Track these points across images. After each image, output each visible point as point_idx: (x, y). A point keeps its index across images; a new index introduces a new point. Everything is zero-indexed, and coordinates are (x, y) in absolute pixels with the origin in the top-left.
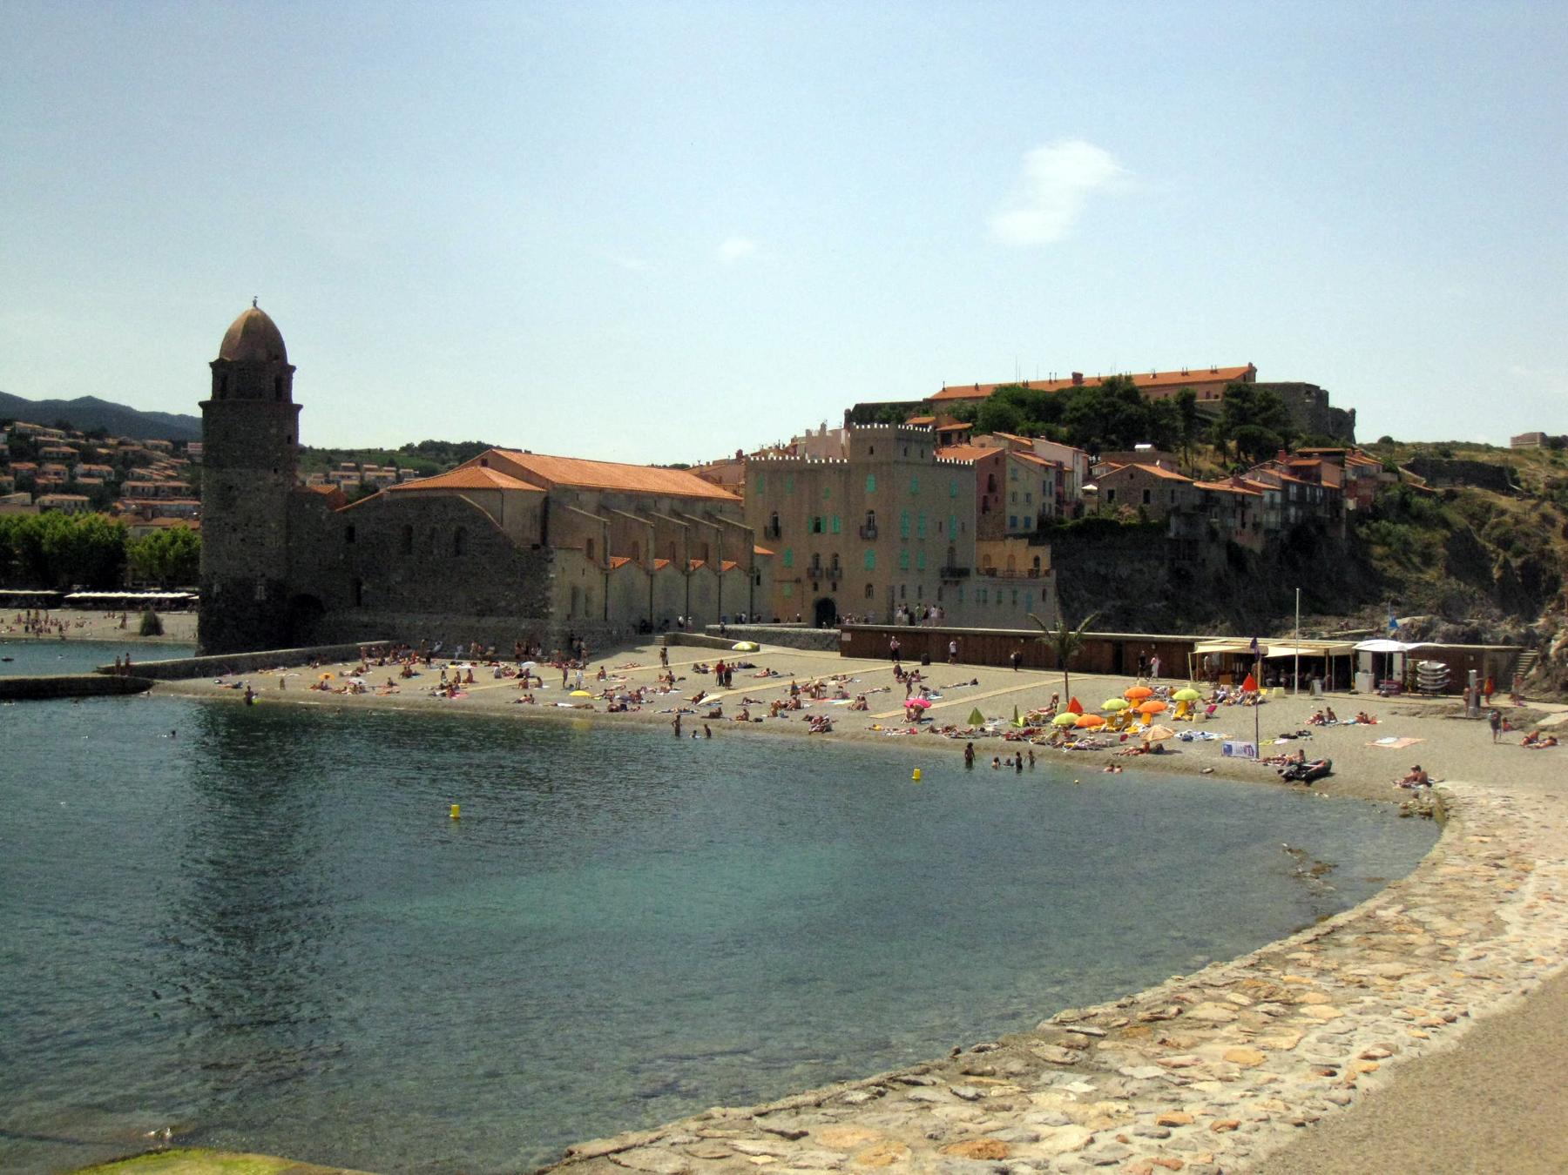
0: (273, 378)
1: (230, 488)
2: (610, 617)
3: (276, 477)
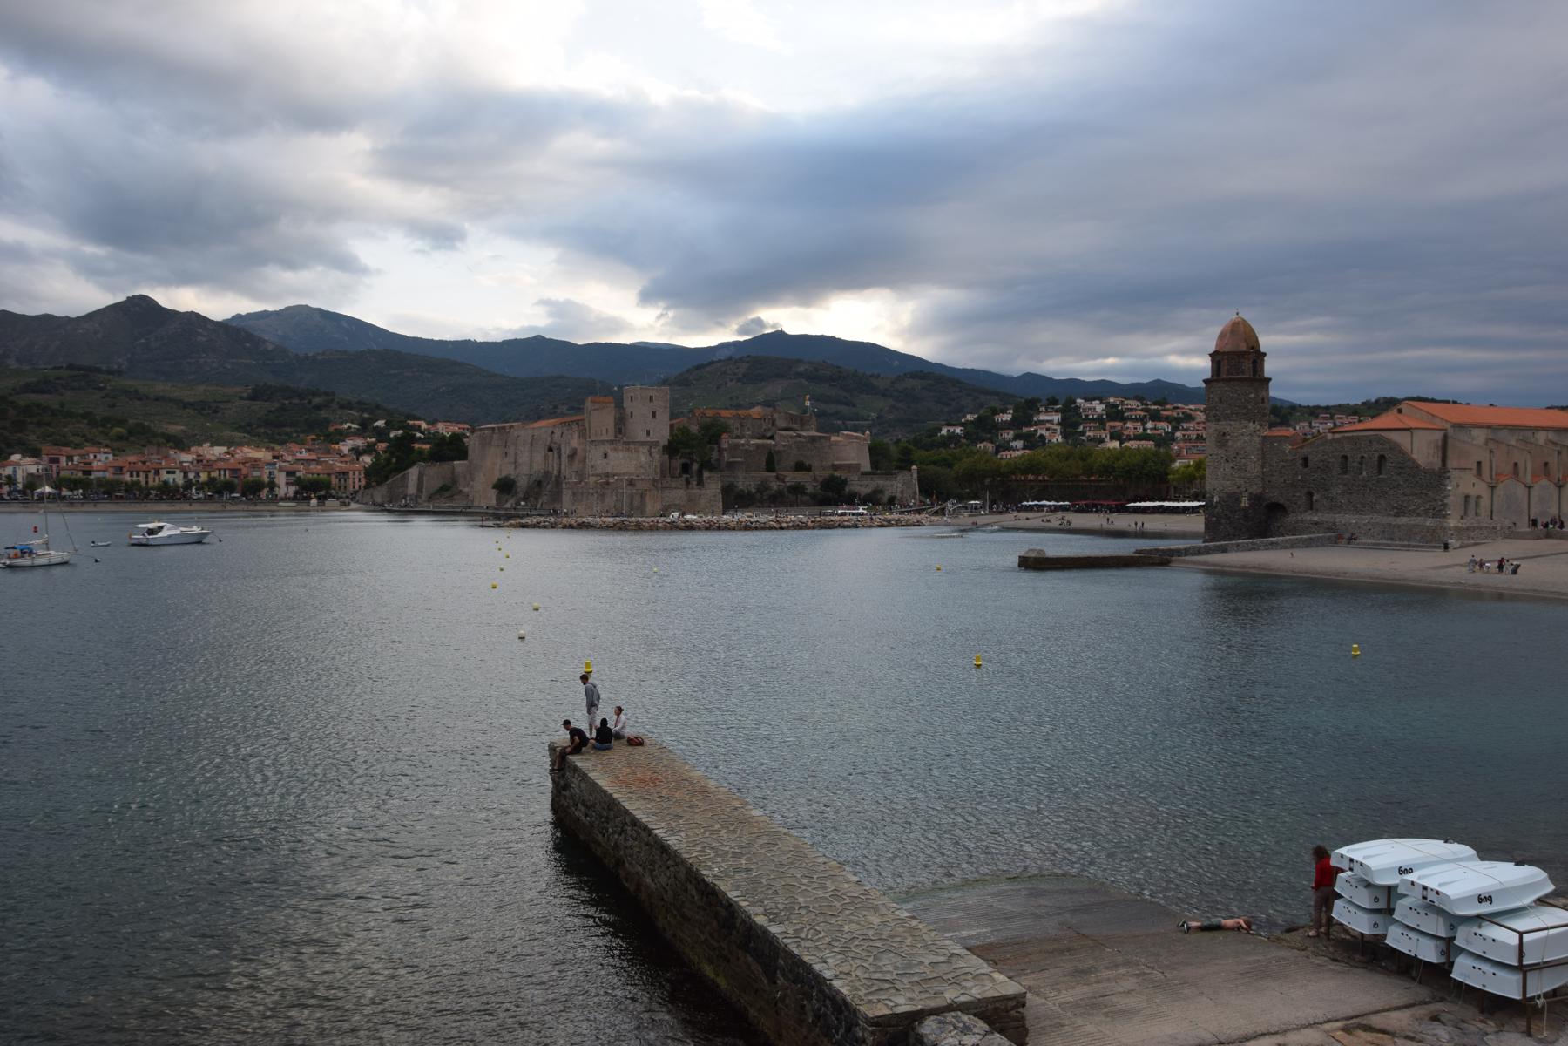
0: (1251, 361)
1: (1224, 434)
2: (1494, 517)
3: (1254, 426)
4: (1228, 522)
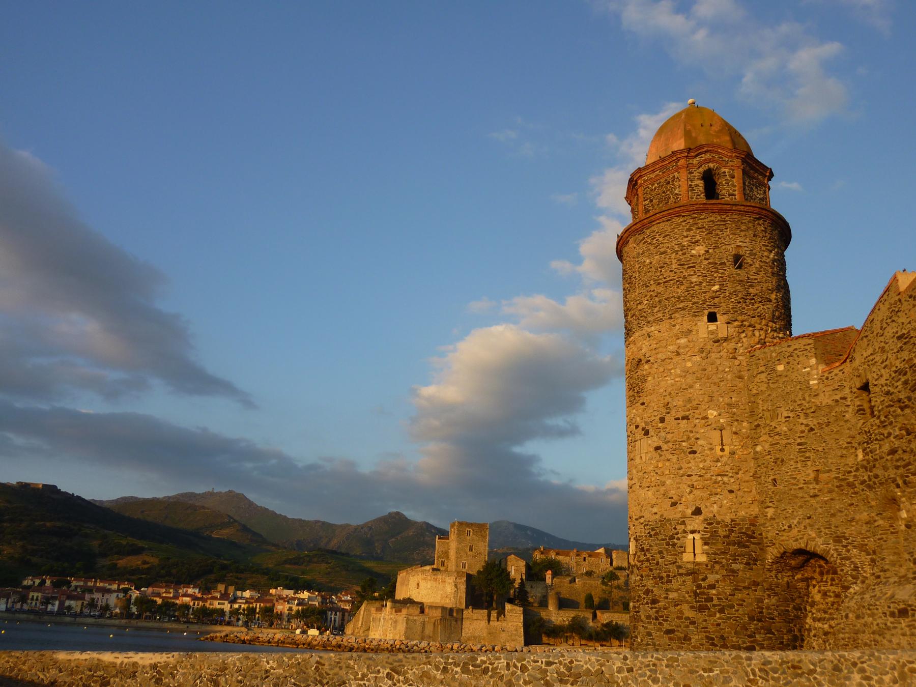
3: (712, 326)
4: (652, 613)
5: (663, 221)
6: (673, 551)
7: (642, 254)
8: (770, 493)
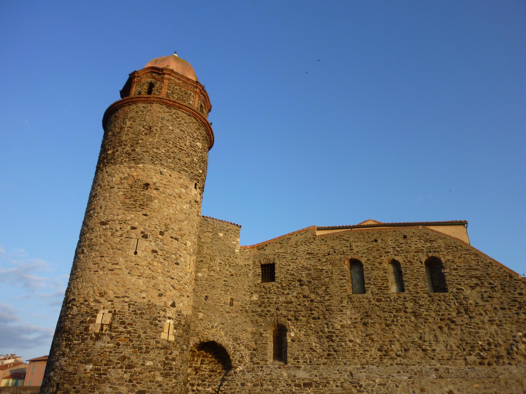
1: (147, 185)
4: (127, 376)
5: (186, 114)
6: (155, 329)
7: (167, 120)
8: (203, 304)
